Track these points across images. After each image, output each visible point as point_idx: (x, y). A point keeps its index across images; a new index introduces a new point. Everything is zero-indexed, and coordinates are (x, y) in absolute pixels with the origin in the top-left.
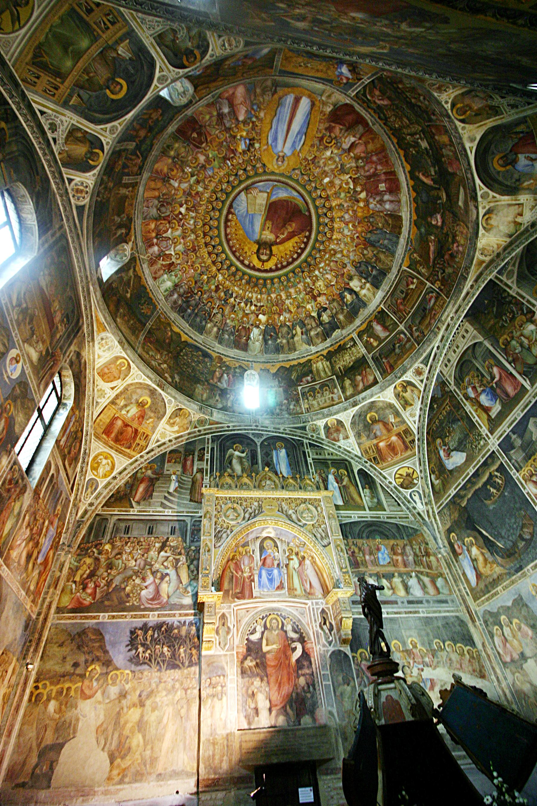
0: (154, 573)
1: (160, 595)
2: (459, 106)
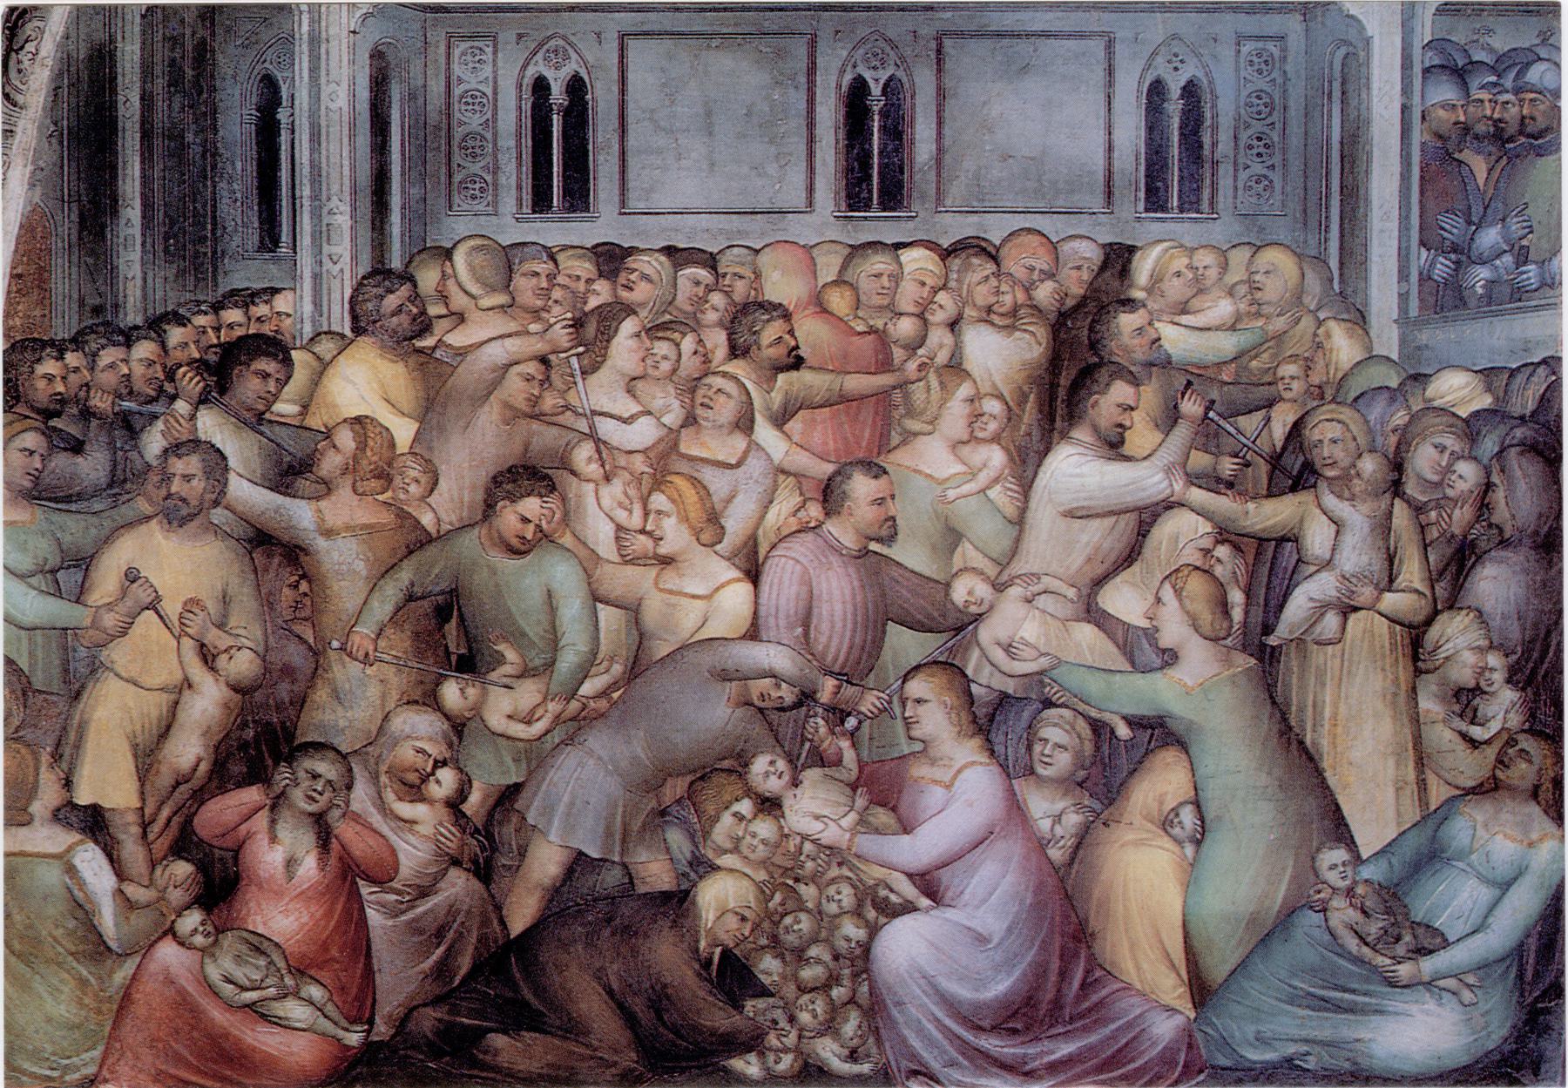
0: (995, 720)
1: (1097, 974)
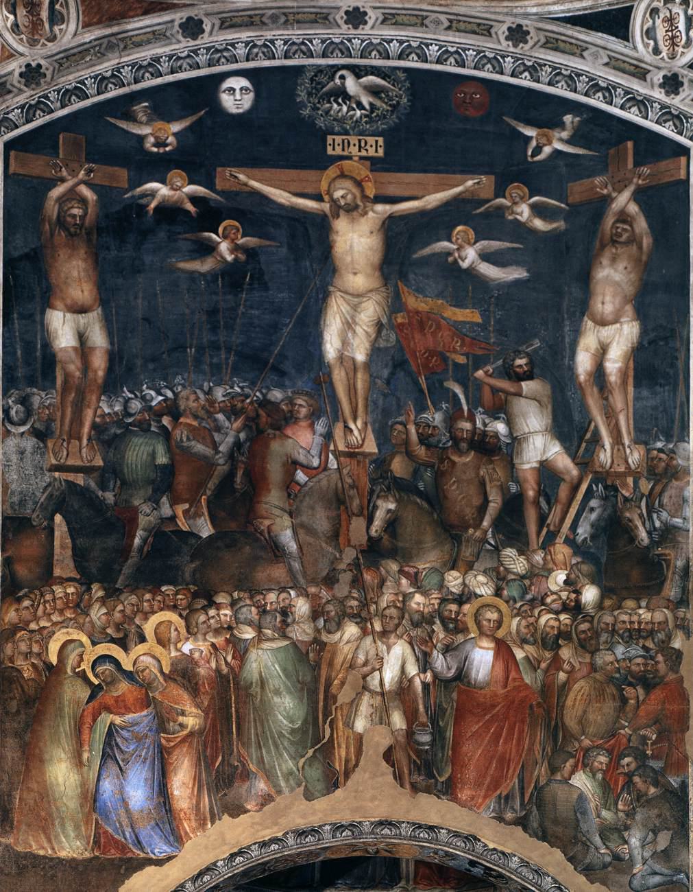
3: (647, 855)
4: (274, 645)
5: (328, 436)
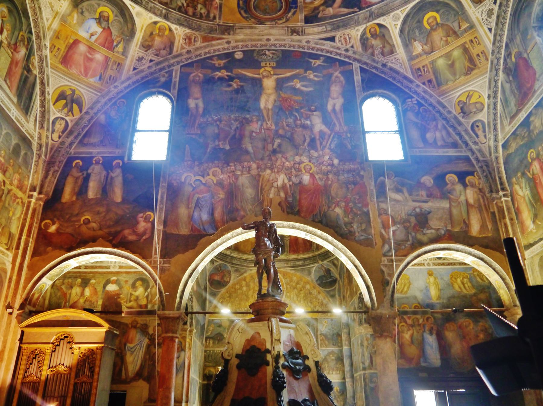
2: (167, 32)
3: (359, 230)
4: (247, 176)
5: (262, 125)
